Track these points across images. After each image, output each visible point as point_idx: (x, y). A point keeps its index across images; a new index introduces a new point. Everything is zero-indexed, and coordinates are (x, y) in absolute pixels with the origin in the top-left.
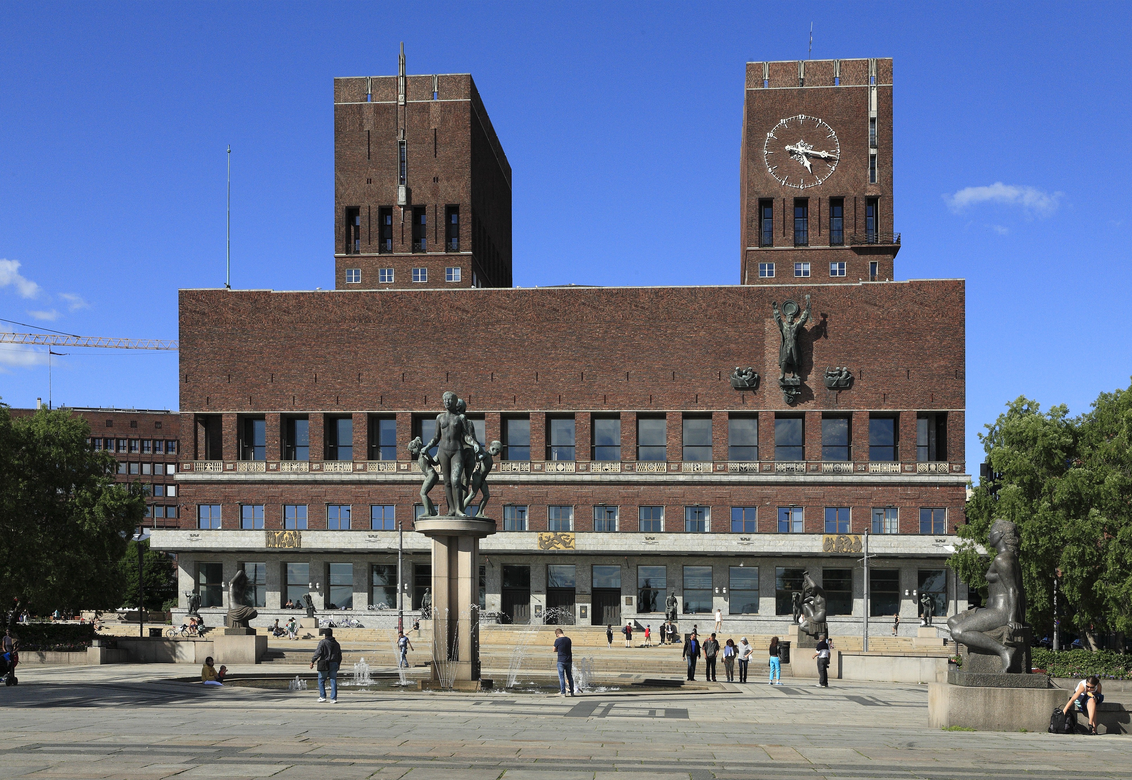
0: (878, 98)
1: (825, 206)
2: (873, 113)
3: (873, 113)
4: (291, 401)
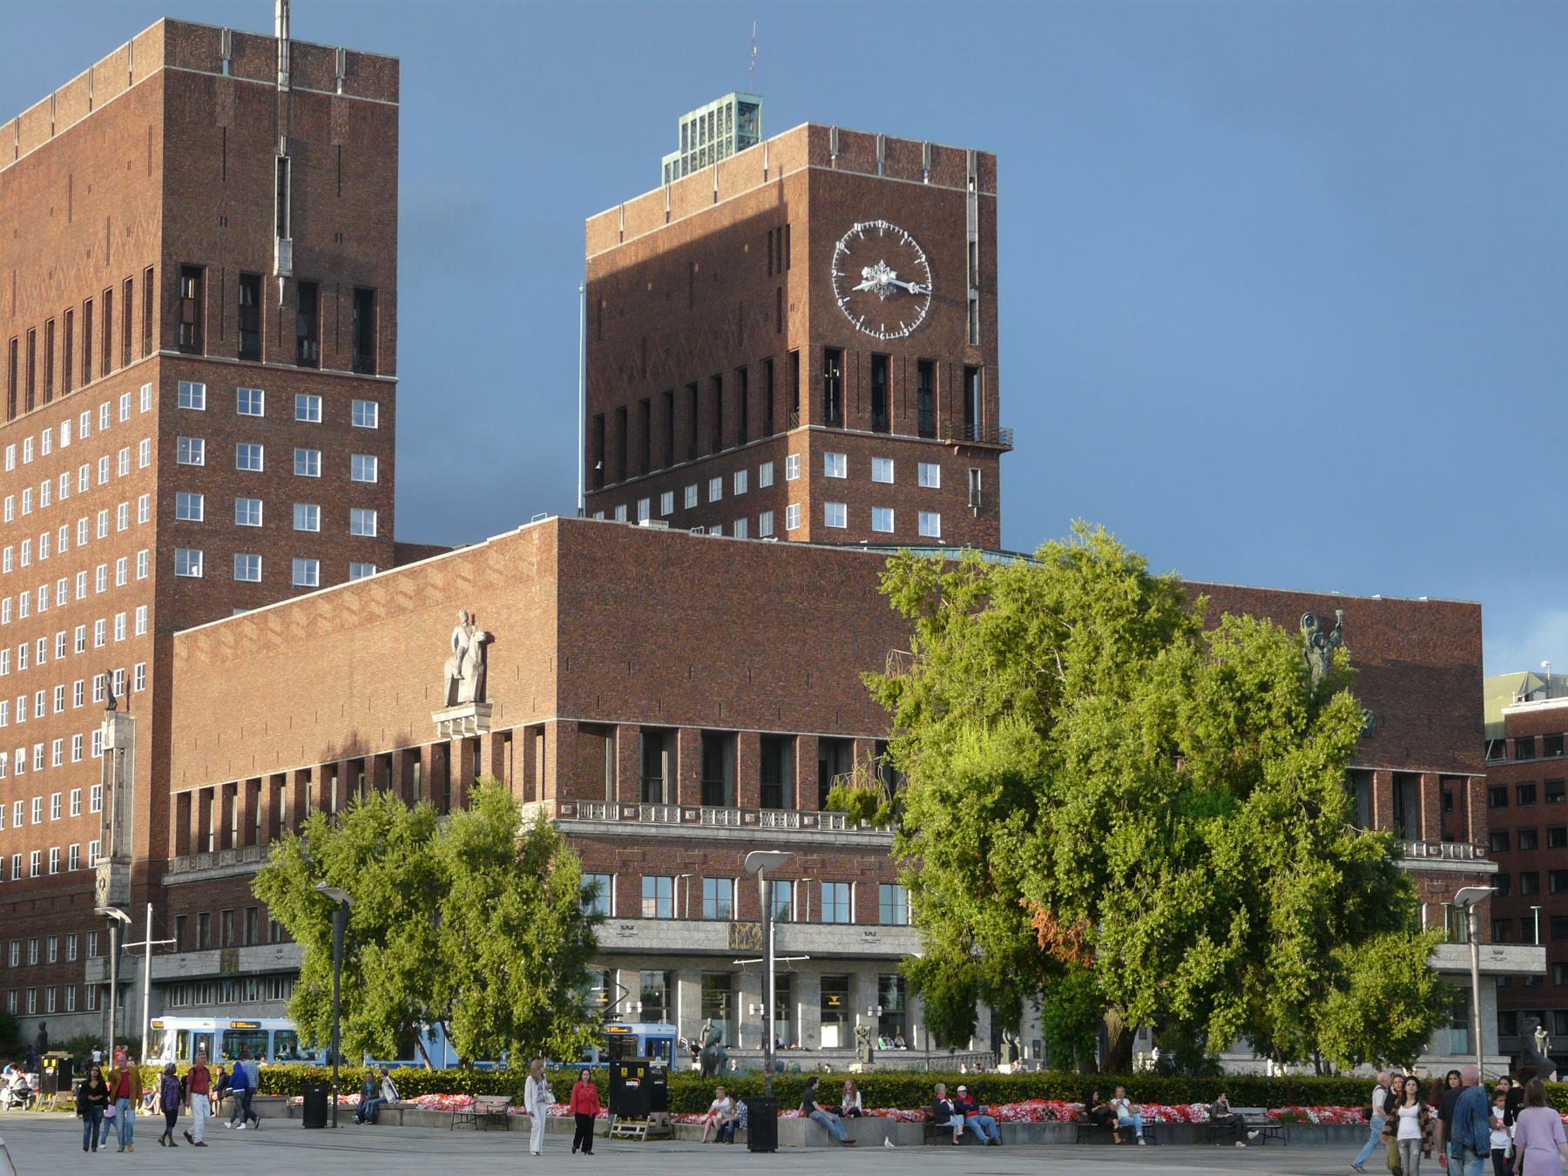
1: (913, 370)
2: (973, 235)
3: (973, 235)
4: (716, 710)
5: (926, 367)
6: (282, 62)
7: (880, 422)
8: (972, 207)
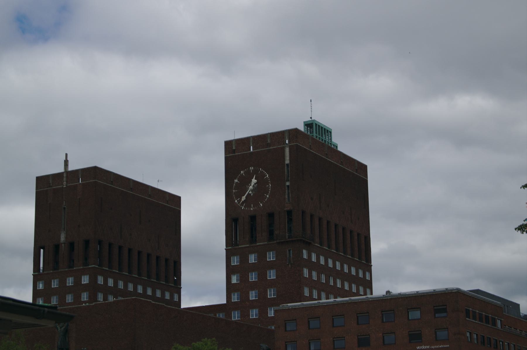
0: (290, 152)
5: (271, 216)
6: (65, 179)
7: (253, 239)
8: (287, 150)
